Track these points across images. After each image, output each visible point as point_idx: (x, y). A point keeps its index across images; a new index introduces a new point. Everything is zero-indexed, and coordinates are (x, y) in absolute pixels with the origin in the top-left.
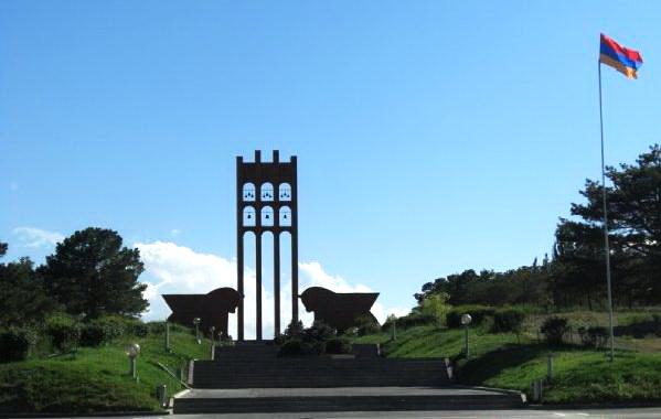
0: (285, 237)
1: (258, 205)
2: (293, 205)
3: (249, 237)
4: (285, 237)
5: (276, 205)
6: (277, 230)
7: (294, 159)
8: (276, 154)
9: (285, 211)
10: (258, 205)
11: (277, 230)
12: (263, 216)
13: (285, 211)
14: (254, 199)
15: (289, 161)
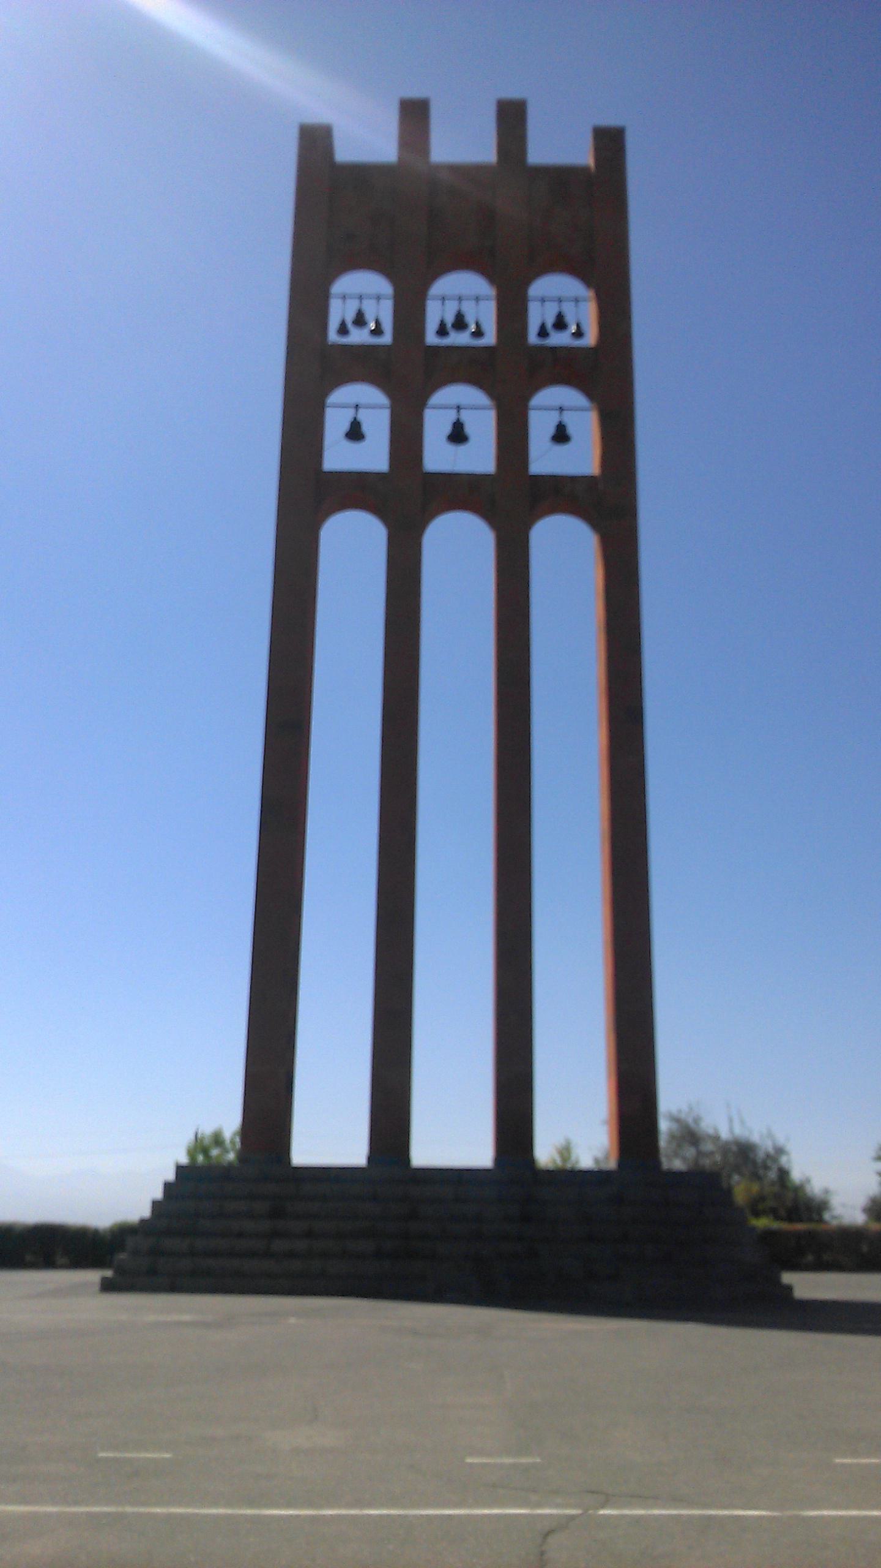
1: (409, 370)
2: (605, 374)
3: (353, 544)
4: (562, 550)
6: (512, 500)
7: (610, 143)
8: (512, 118)
10: (409, 370)
11: (512, 500)
12: (435, 424)
14: (387, 339)
15: (583, 155)
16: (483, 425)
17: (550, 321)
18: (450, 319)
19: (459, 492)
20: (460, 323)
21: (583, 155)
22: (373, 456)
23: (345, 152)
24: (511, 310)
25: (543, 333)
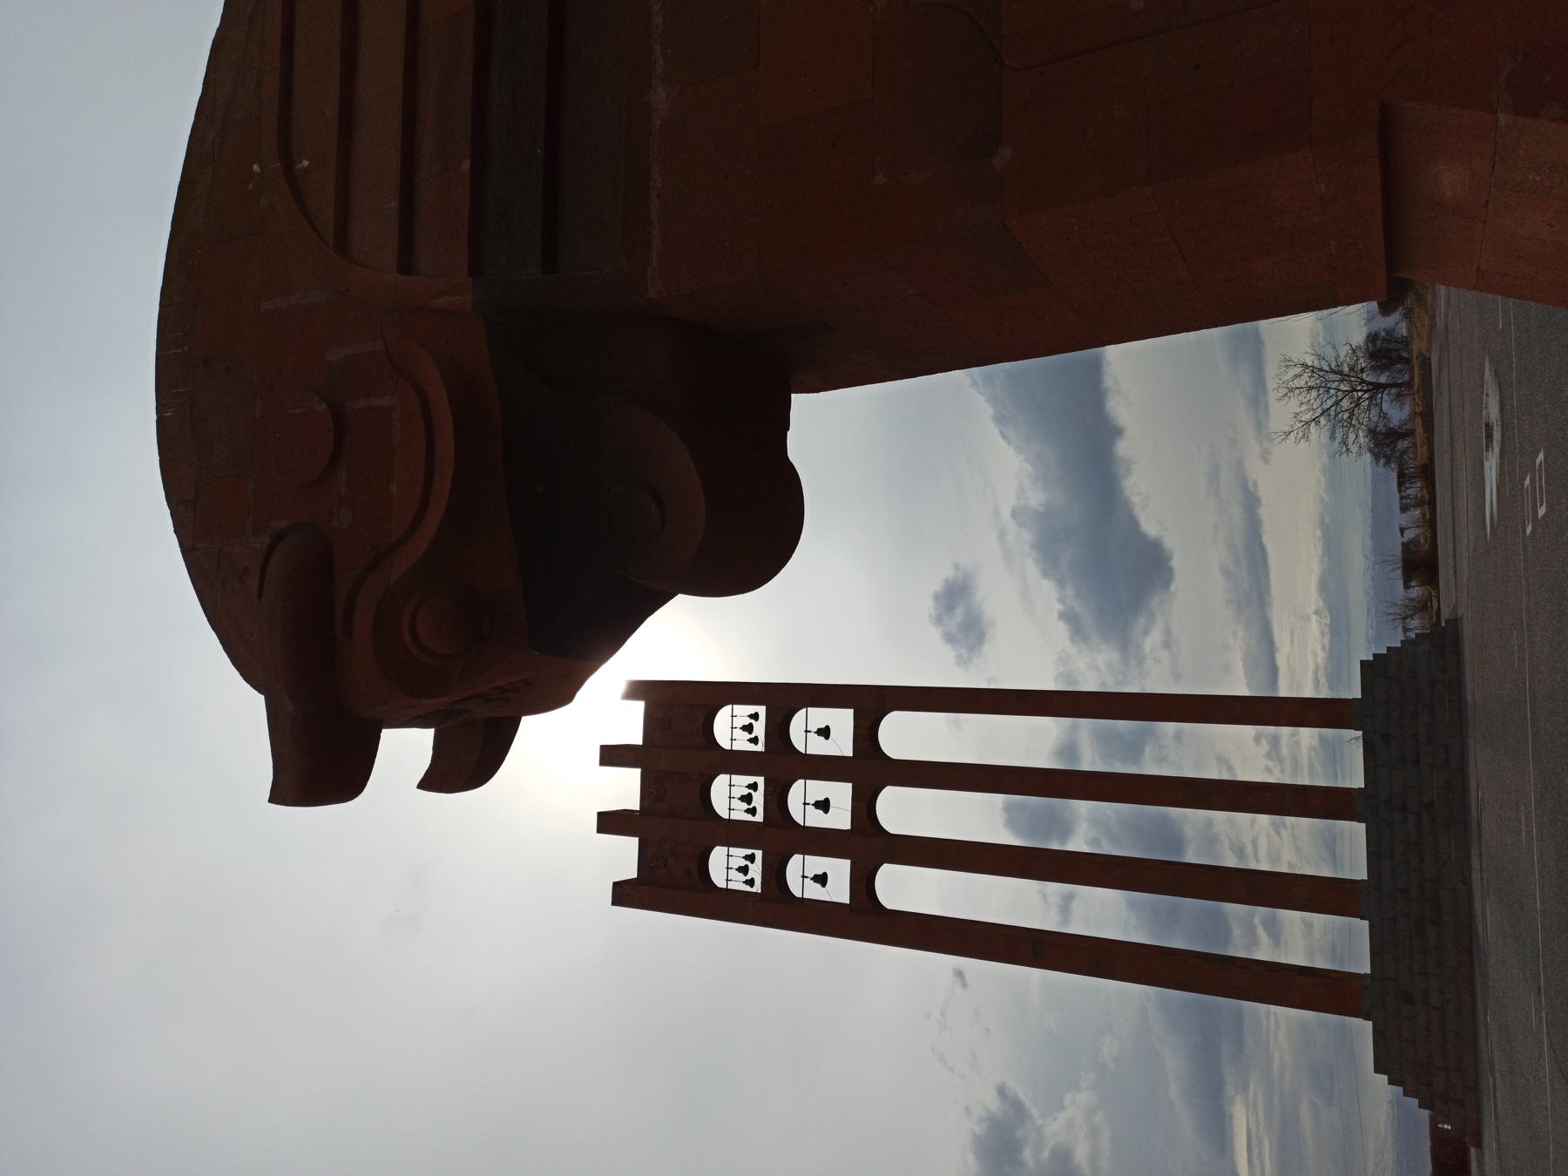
0: (903, 736)
2: (783, 700)
5: (780, 764)
6: (870, 770)
8: (612, 756)
9: (803, 729)
10: (779, 836)
11: (870, 770)
13: (803, 729)
16: (818, 789)
17: (747, 736)
18: (745, 806)
19: (864, 807)
20: (747, 799)
21: (639, 707)
22: (839, 870)
23: (632, 873)
24: (737, 762)
25: (755, 741)
